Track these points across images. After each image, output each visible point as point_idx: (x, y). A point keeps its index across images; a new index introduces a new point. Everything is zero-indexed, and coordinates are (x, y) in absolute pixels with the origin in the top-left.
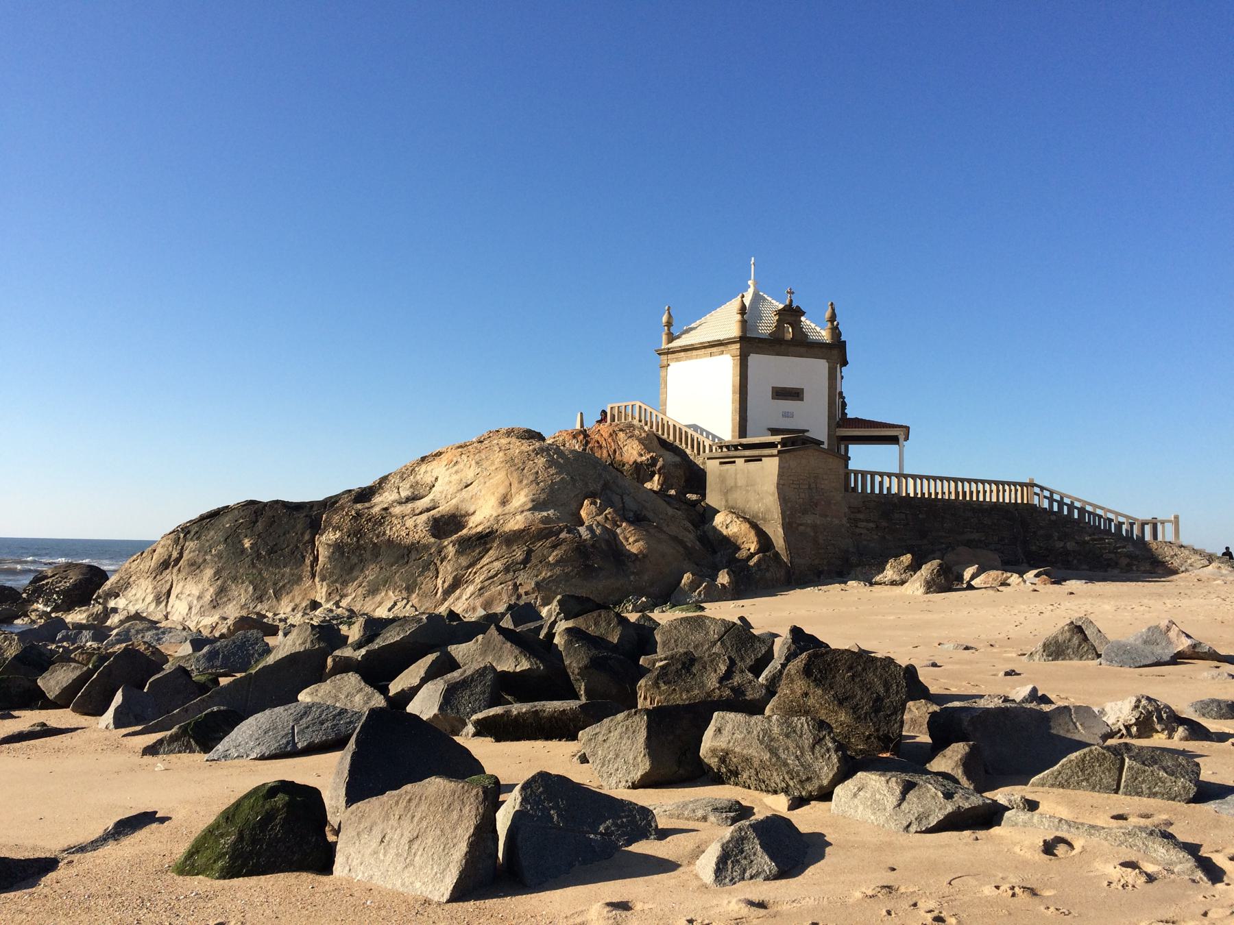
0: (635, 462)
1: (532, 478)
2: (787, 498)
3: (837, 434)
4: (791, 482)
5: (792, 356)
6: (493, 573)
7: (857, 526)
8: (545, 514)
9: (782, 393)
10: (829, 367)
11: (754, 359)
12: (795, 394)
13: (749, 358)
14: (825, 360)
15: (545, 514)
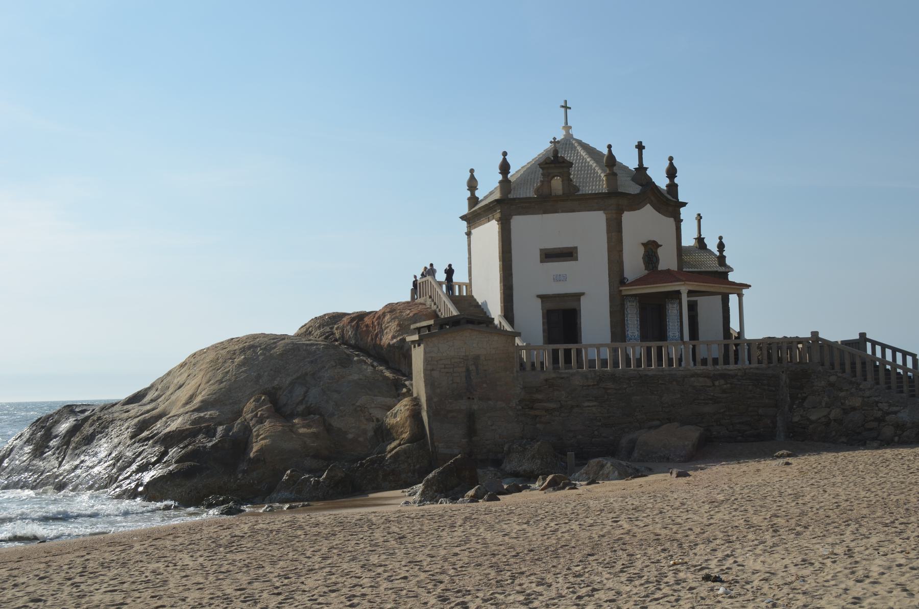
0: (389, 343)
1: (219, 377)
2: (436, 384)
3: (624, 293)
4: (443, 366)
5: (563, 212)
6: (129, 473)
7: (532, 408)
8: (202, 415)
9: (549, 256)
10: (607, 219)
11: (518, 222)
12: (568, 254)
13: (512, 221)
14: (602, 212)
15: (202, 415)
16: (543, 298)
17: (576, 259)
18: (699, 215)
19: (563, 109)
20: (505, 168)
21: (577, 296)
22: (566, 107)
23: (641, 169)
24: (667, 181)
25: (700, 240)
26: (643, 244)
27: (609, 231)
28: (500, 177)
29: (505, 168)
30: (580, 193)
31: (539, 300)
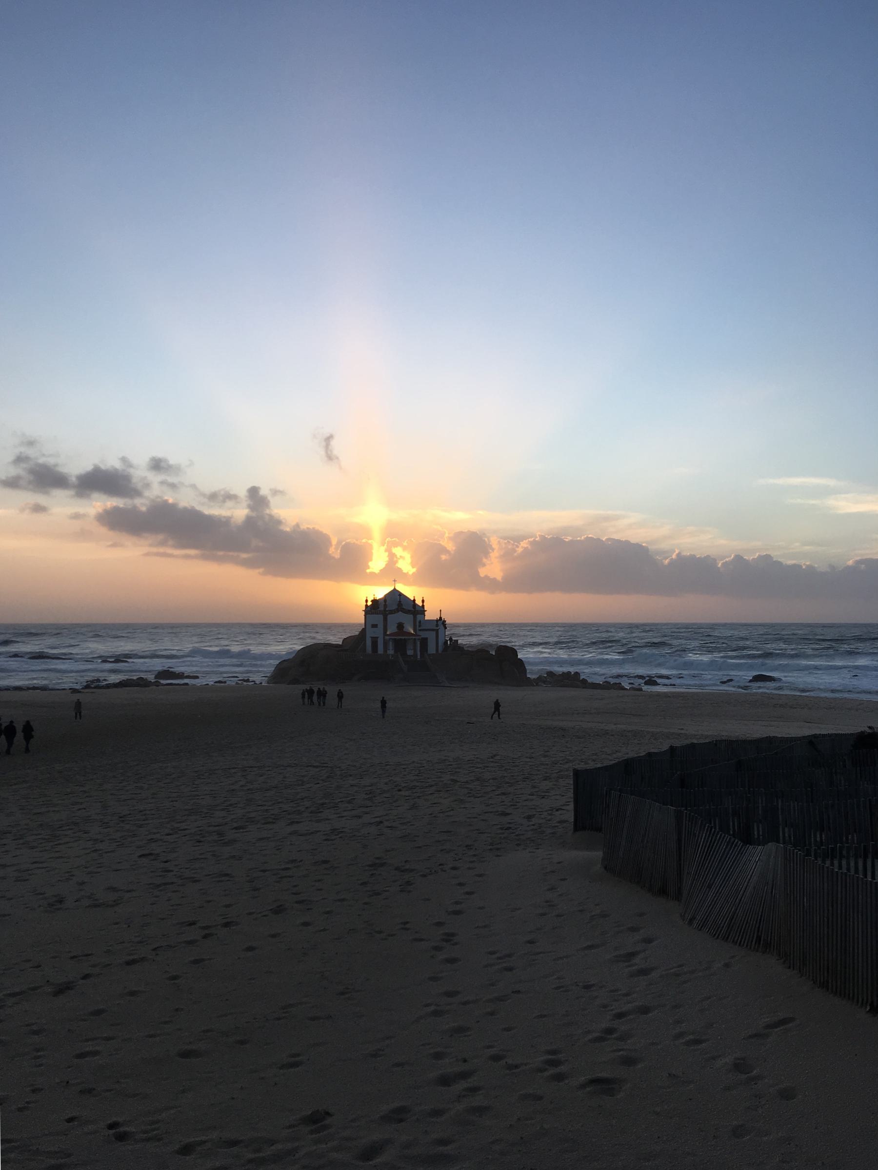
16: (371, 637)
17: (377, 627)
18: (441, 611)
19: (394, 582)
20: (367, 601)
21: (377, 638)
22: (395, 581)
23: (400, 602)
24: (413, 603)
25: (441, 618)
26: (398, 624)
27: (384, 620)
28: (365, 604)
29: (367, 601)
30: (379, 609)
31: (370, 639)
